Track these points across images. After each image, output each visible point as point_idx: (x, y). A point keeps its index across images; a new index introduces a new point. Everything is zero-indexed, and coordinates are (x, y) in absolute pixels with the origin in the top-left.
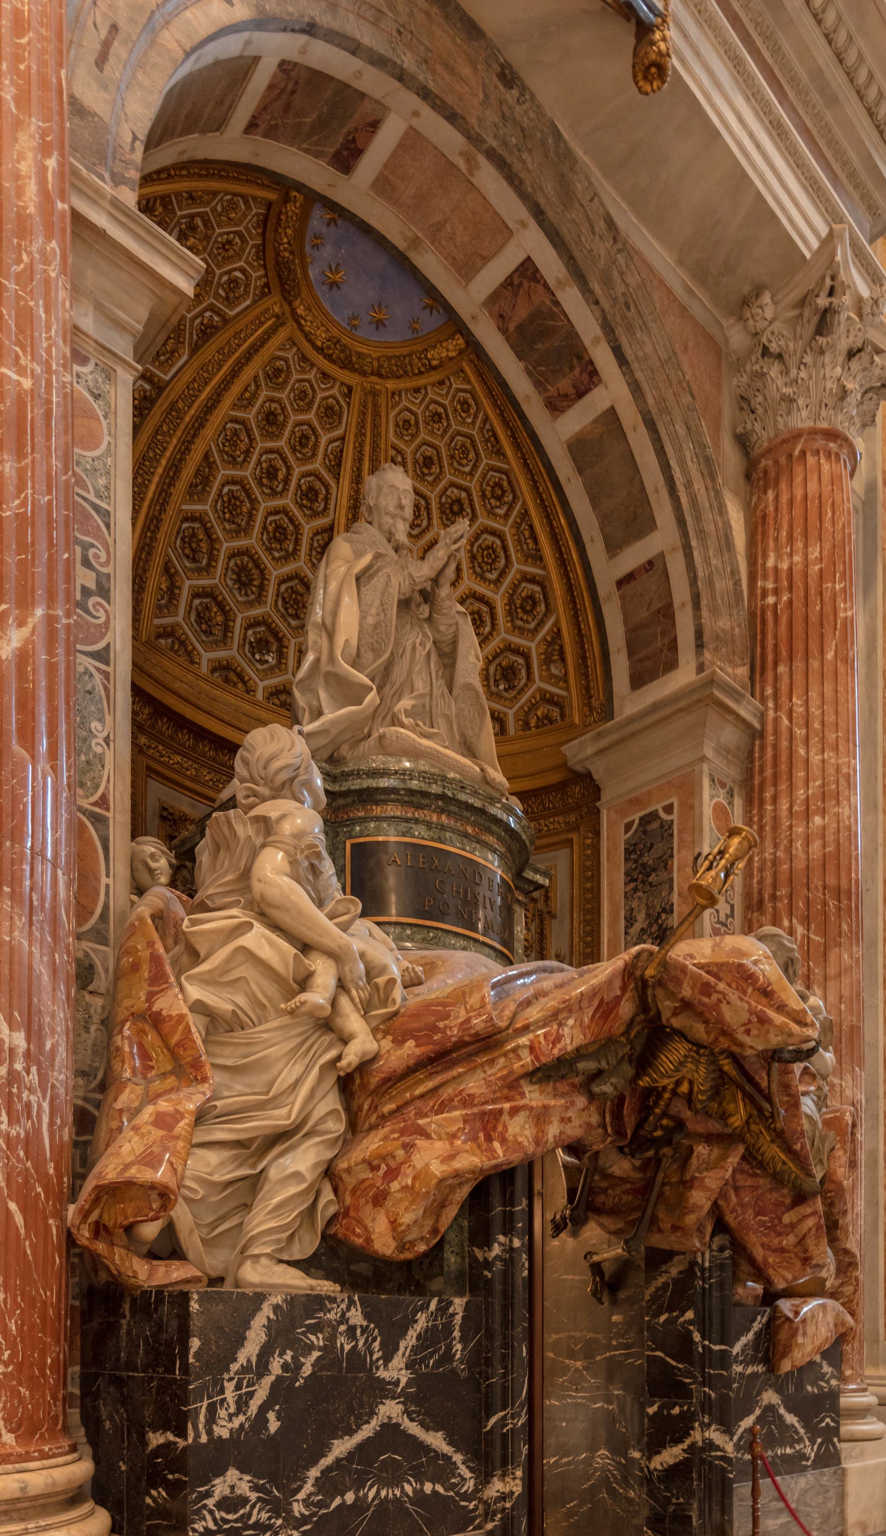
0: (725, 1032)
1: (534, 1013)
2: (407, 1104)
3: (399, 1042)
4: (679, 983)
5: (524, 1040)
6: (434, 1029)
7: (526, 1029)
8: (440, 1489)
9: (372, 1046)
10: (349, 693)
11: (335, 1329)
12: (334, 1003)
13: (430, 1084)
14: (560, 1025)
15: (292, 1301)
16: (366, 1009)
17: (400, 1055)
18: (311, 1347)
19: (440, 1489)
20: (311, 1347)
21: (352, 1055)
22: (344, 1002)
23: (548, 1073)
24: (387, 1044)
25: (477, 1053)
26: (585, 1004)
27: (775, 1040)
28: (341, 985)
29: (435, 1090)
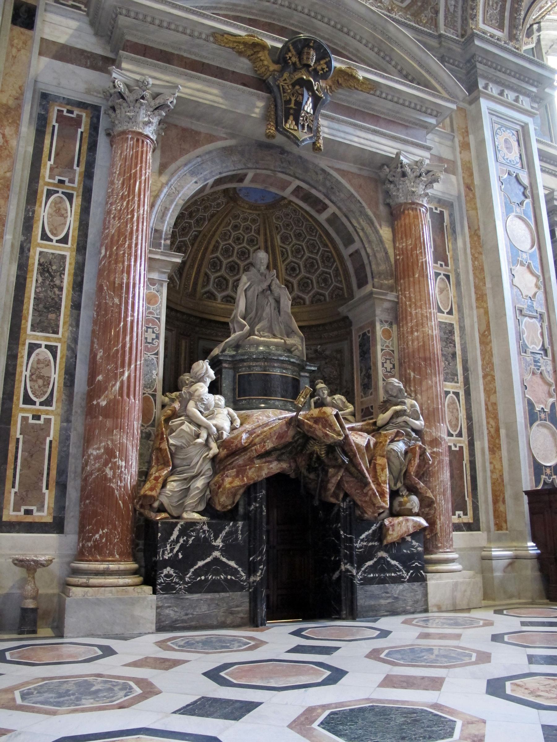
0: (320, 438)
1: (257, 440)
2: (226, 466)
3: (223, 449)
4: (303, 425)
5: (253, 448)
6: (230, 446)
7: (255, 444)
8: (233, 578)
9: (217, 451)
10: (242, 327)
11: (199, 530)
12: (207, 440)
13: (231, 461)
14: (265, 442)
15: (187, 523)
16: (216, 440)
17: (224, 452)
18: (192, 536)
19: (233, 578)
20: (192, 536)
21: (211, 453)
22: (210, 440)
23: (261, 456)
24: (221, 450)
25: (242, 452)
26: (272, 435)
27: (332, 440)
28: (209, 435)
29: (232, 462)
